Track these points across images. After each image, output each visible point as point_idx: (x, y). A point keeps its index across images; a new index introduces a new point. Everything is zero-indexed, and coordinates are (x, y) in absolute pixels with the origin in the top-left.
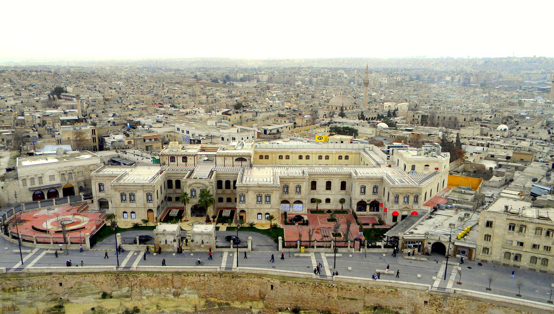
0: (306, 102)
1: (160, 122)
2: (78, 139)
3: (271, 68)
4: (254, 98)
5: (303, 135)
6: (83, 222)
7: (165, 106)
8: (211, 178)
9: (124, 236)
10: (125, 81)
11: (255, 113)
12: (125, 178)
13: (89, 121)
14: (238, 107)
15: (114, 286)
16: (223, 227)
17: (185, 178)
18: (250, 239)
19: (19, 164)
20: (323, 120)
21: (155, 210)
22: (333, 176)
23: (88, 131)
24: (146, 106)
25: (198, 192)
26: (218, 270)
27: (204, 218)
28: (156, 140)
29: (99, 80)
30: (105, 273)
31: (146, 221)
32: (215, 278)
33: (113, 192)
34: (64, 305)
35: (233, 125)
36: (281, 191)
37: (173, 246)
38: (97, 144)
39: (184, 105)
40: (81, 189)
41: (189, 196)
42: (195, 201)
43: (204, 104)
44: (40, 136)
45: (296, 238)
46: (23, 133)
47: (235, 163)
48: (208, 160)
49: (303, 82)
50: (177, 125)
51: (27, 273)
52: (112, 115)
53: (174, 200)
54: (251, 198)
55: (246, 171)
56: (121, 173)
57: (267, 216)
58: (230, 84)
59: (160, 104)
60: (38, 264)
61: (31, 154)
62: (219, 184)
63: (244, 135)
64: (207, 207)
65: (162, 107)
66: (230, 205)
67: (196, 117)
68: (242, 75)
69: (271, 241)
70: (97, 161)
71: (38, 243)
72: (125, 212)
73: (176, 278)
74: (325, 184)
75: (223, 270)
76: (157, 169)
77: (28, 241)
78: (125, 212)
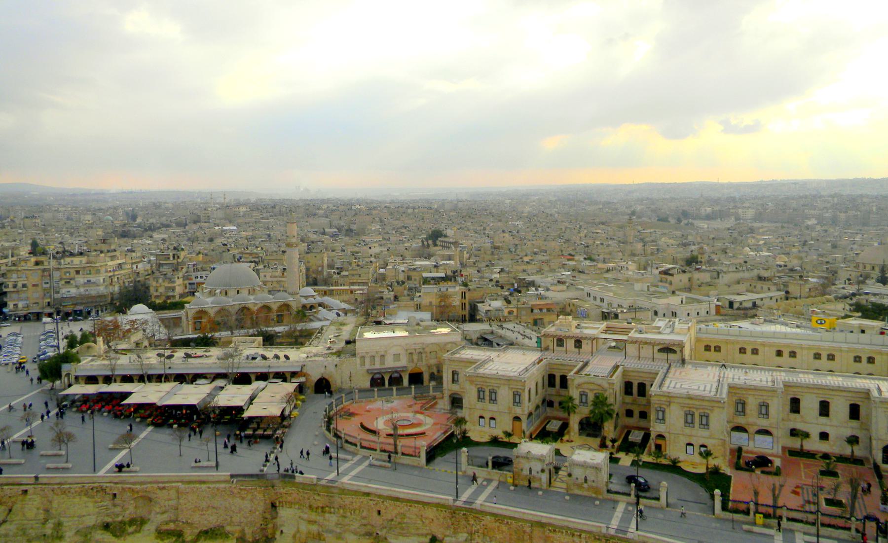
0: (819, 255)
1: (563, 283)
2: (443, 304)
3: (764, 197)
4: (724, 247)
5: (799, 315)
6: (426, 424)
7: (576, 258)
8: (612, 376)
9: (471, 453)
10: (527, 220)
11: (715, 274)
12: (486, 366)
13: (459, 279)
14: (692, 261)
15: (448, 527)
16: (626, 460)
17: (572, 373)
18: (664, 485)
19: (360, 336)
20: (843, 288)
21: (524, 418)
22: (833, 393)
23: (456, 293)
24: (548, 258)
25: (591, 397)
26: (604, 531)
27: (598, 440)
28: (548, 310)
29: (492, 219)
30: (439, 505)
31: (508, 435)
33: (467, 385)
35: (673, 292)
36: (732, 410)
37: (541, 479)
38: (466, 312)
39: (606, 256)
40: (433, 377)
41: (577, 402)
42: (584, 411)
43: (638, 255)
44: (396, 298)
45: (747, 496)
46: (376, 293)
47: (658, 355)
48: (614, 347)
49: (820, 220)
50: (587, 289)
51: (340, 489)
52: (498, 270)
53: (556, 408)
54: (675, 416)
55: (672, 370)
56: (484, 358)
57: (703, 449)
58: (687, 224)
59: (570, 255)
60: (357, 477)
61: (378, 323)
62: (628, 387)
63: (693, 308)
64: (602, 422)
65: (572, 260)
66: (643, 423)
67: (620, 276)
68: (709, 210)
69: (704, 494)
70: (457, 338)
71: (362, 447)
72: (481, 417)
73: (537, 532)
74: (817, 406)
75: (613, 532)
76: (534, 356)
77: (351, 443)
78: (481, 417)
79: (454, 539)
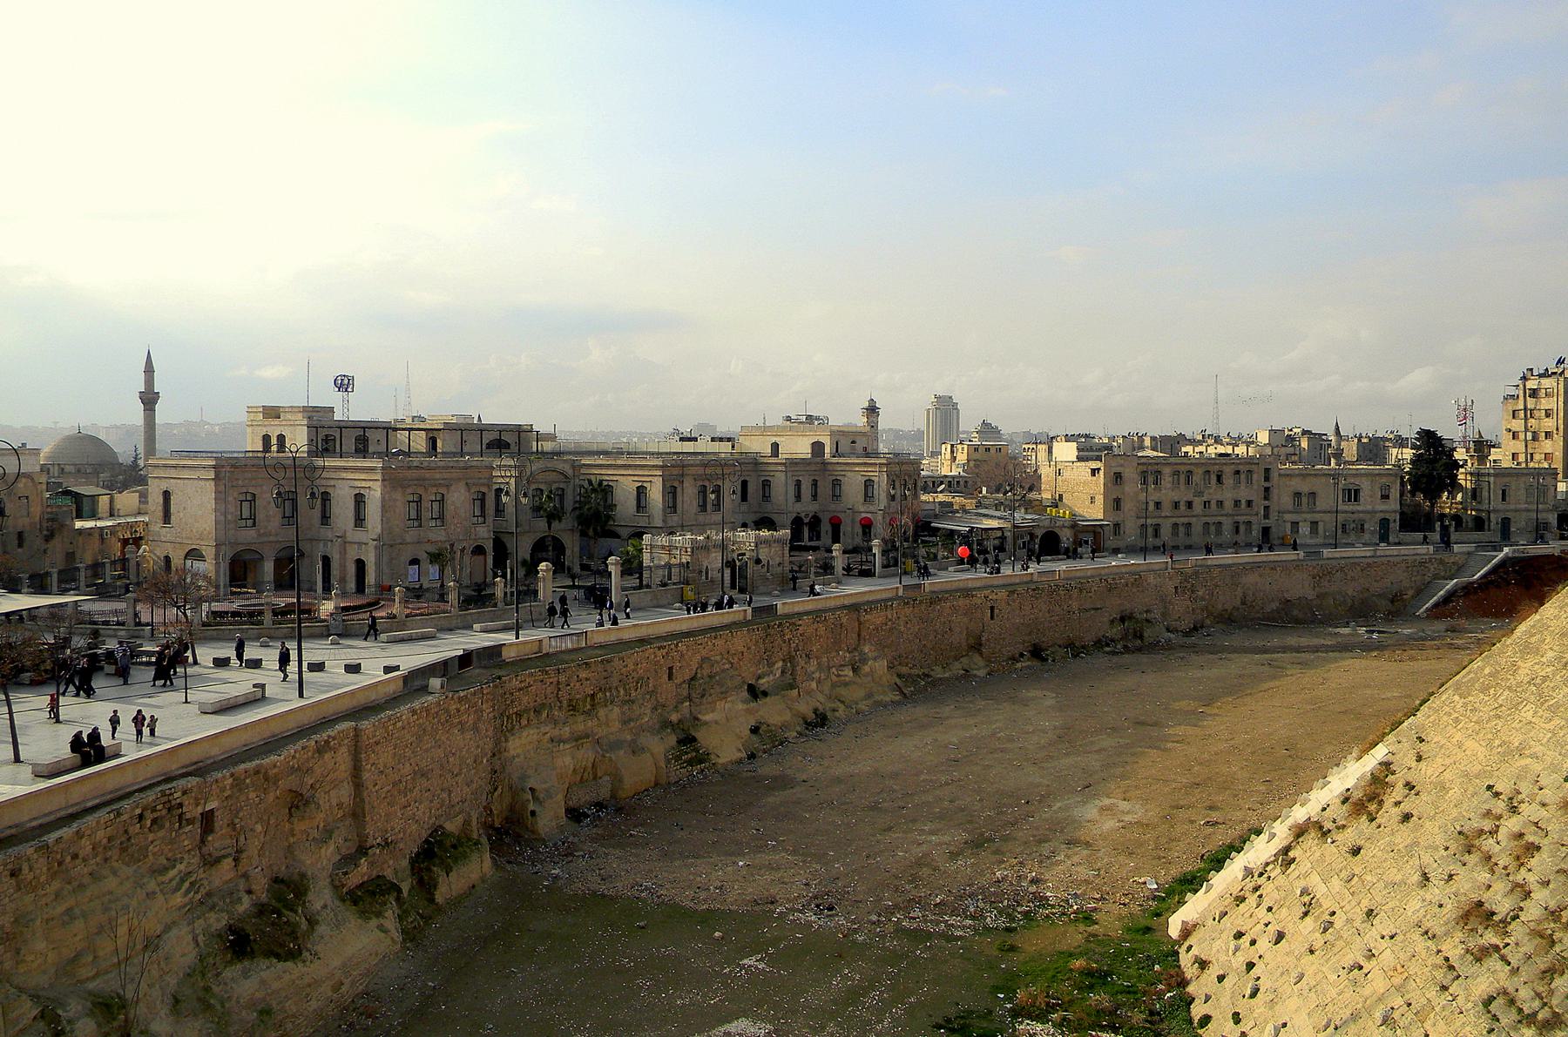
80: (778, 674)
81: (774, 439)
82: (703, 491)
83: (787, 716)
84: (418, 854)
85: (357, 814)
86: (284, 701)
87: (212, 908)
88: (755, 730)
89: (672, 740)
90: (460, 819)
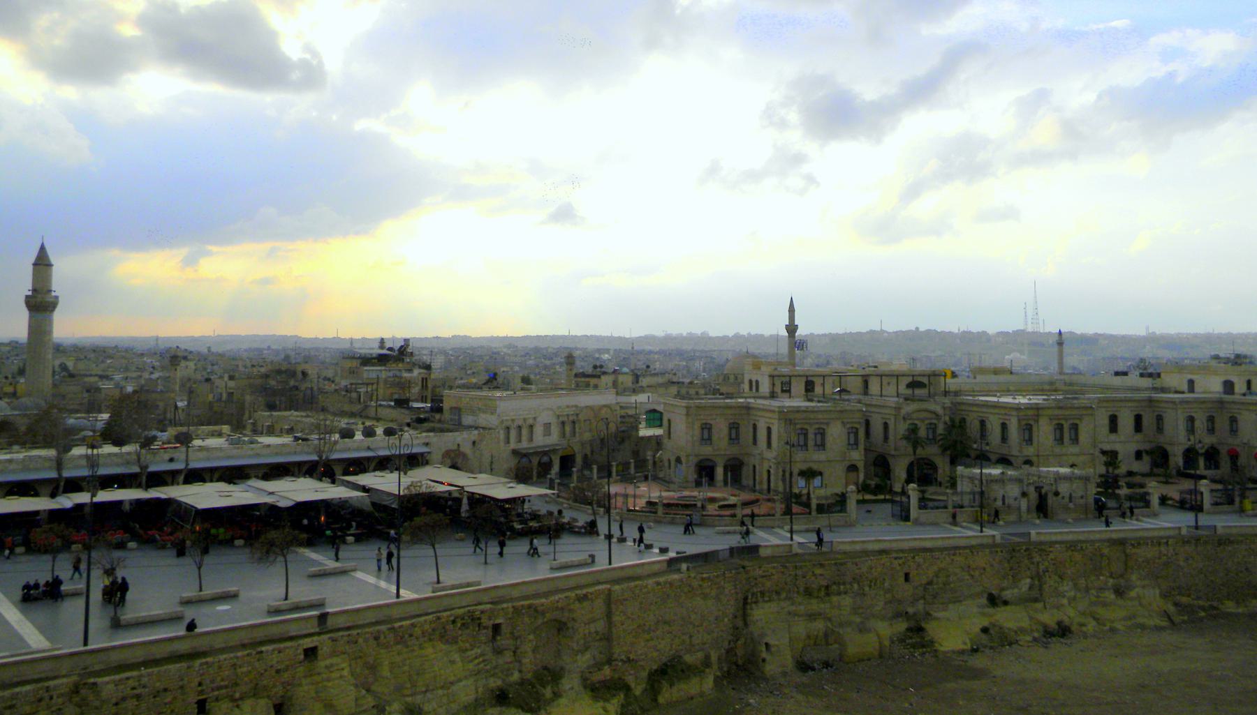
15: (1004, 577)
32: (1187, 547)
34: (923, 625)
79: (1016, 590)
80: (1025, 589)
81: (1190, 377)
82: (1060, 427)
83: (1025, 623)
84: (656, 671)
85: (607, 638)
86: (601, 564)
87: (493, 675)
88: (985, 630)
89: (902, 626)
90: (700, 655)
